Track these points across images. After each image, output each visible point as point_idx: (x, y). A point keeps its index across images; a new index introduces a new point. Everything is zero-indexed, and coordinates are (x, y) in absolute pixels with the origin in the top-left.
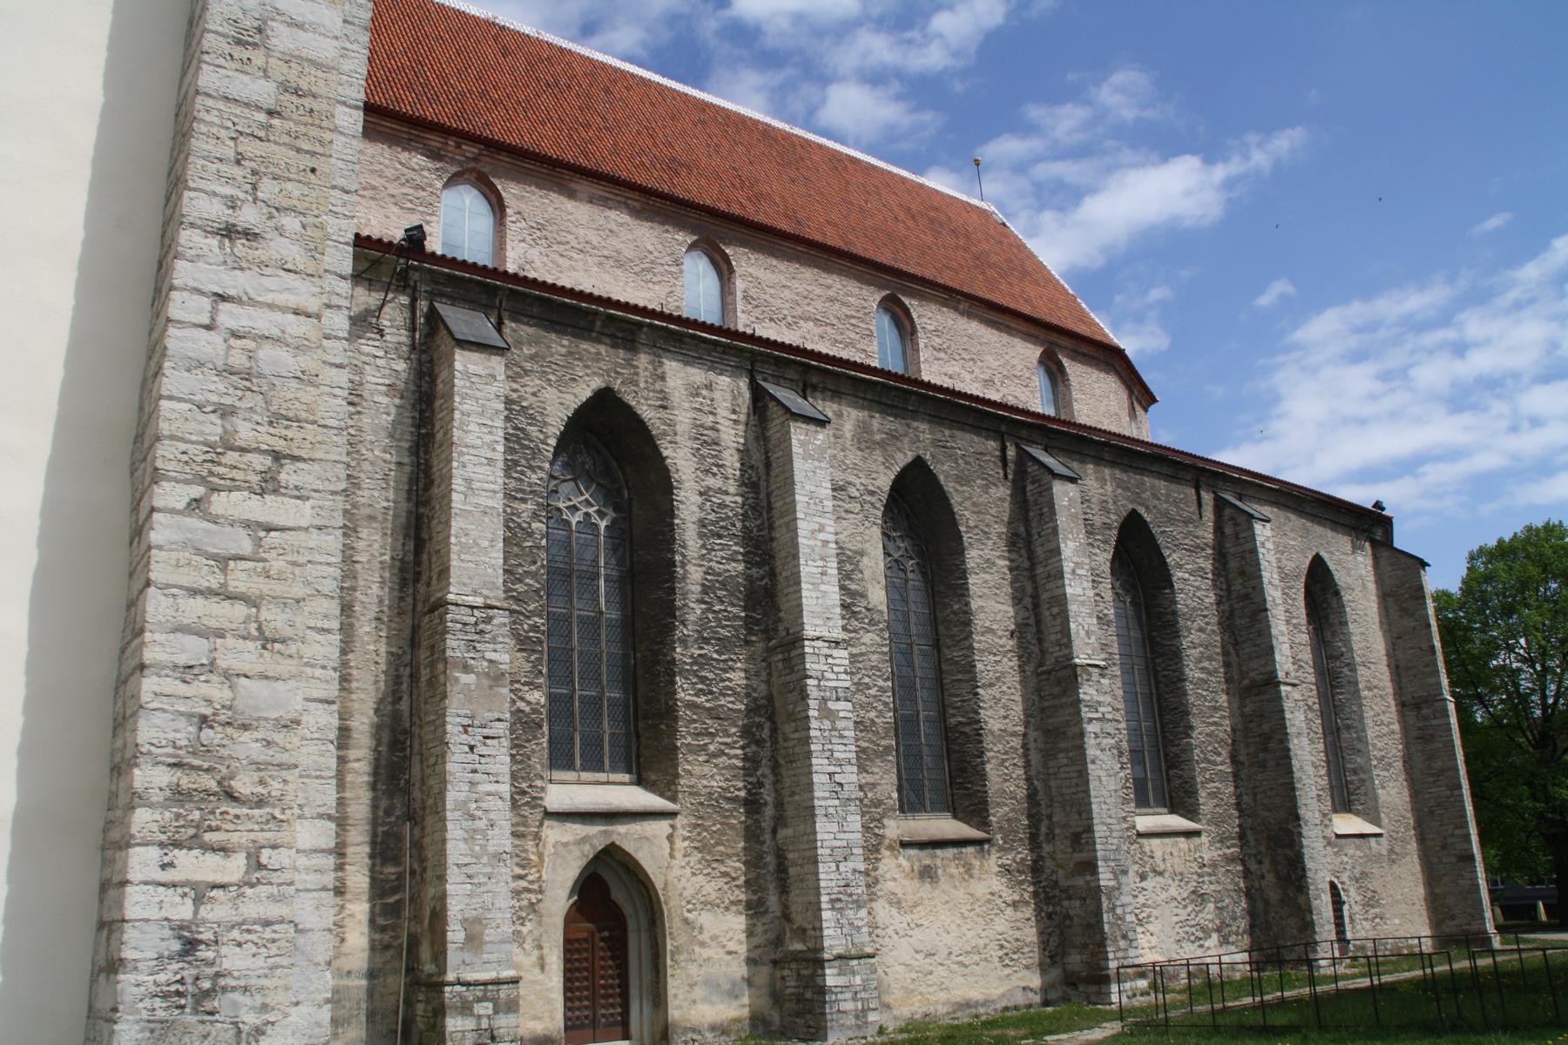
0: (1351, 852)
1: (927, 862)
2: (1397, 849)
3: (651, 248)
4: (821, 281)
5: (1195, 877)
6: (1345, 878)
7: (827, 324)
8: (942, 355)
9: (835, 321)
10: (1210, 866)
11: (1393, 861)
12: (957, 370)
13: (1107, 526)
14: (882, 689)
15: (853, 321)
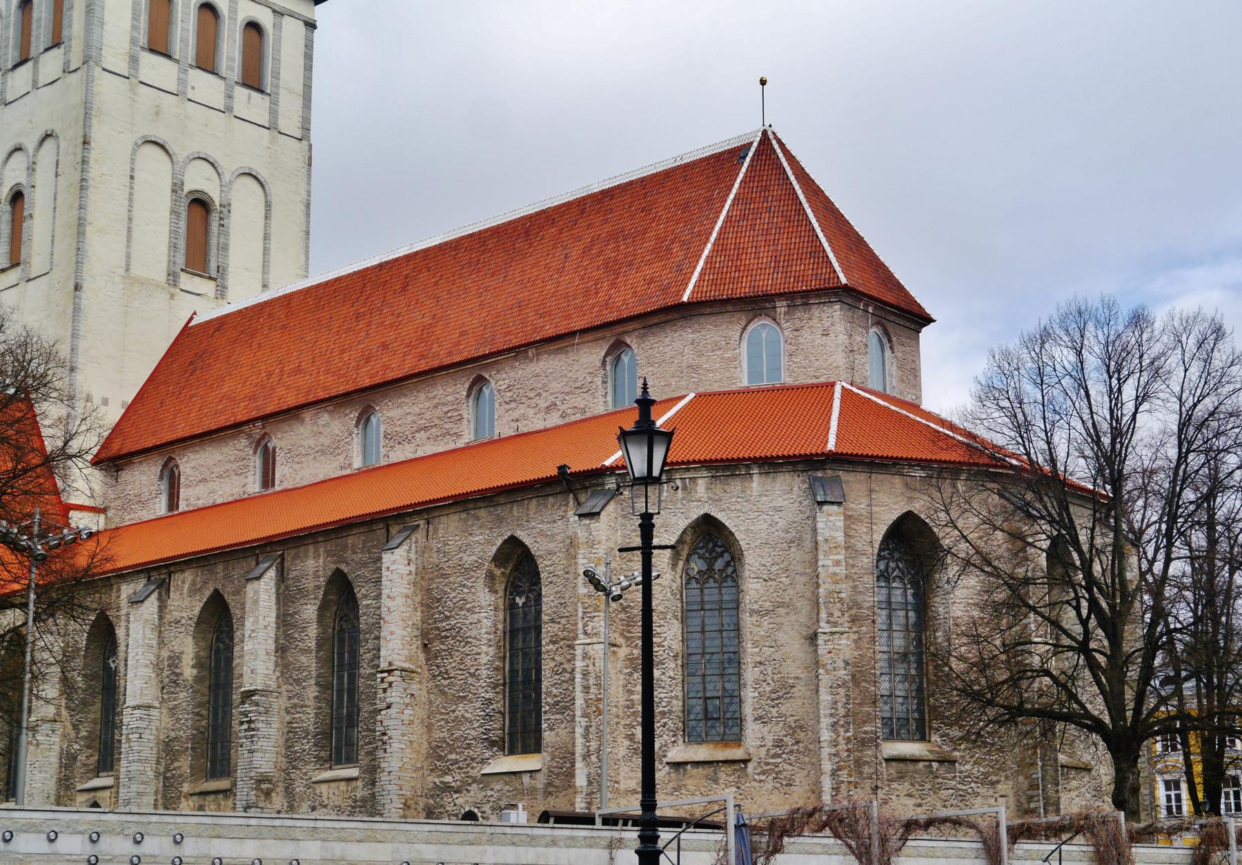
0: (498, 787)
1: (202, 803)
2: (557, 782)
3: (337, 432)
4: (431, 395)
5: (349, 808)
6: (487, 808)
7: (432, 427)
8: (513, 405)
9: (437, 421)
10: (361, 801)
11: (550, 793)
12: (522, 411)
13: (318, 587)
14: (187, 720)
15: (449, 415)
